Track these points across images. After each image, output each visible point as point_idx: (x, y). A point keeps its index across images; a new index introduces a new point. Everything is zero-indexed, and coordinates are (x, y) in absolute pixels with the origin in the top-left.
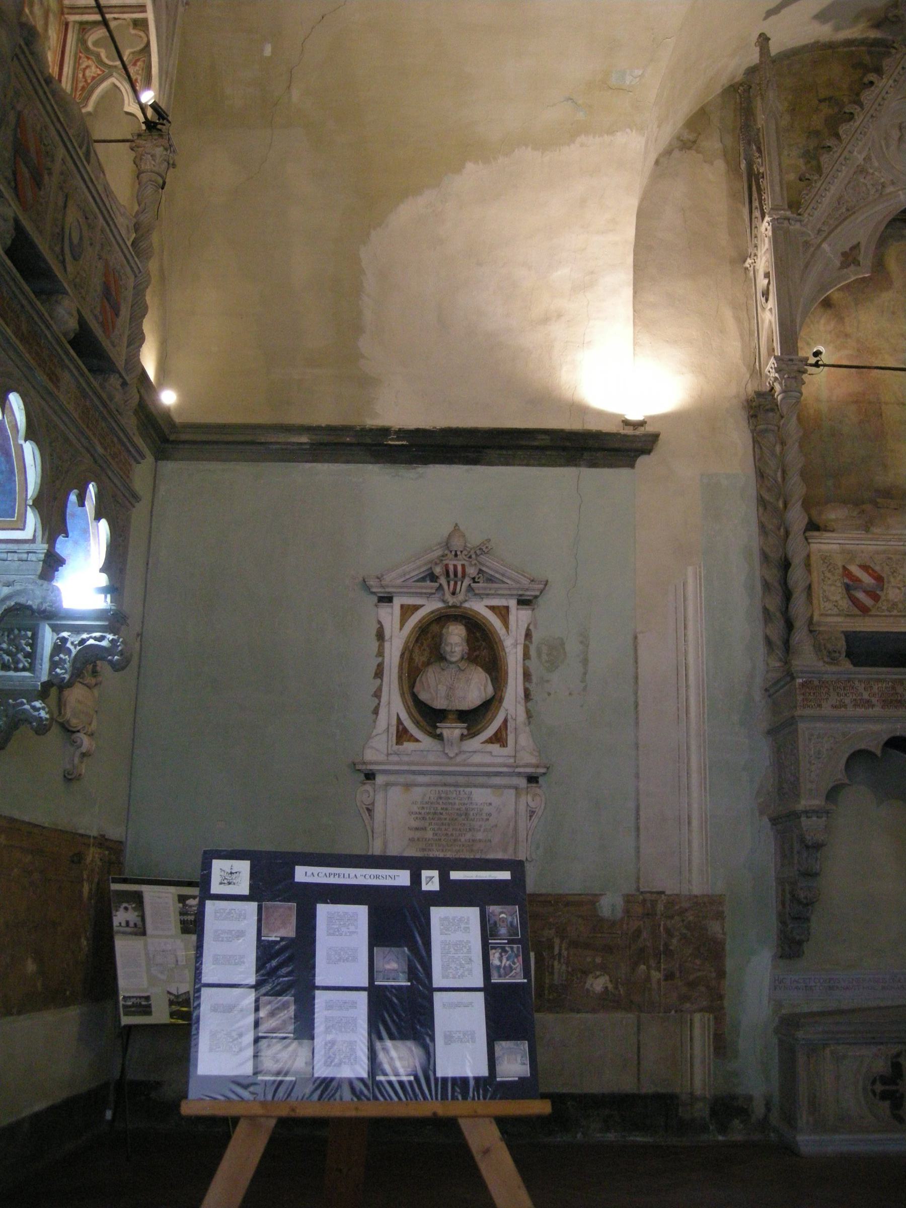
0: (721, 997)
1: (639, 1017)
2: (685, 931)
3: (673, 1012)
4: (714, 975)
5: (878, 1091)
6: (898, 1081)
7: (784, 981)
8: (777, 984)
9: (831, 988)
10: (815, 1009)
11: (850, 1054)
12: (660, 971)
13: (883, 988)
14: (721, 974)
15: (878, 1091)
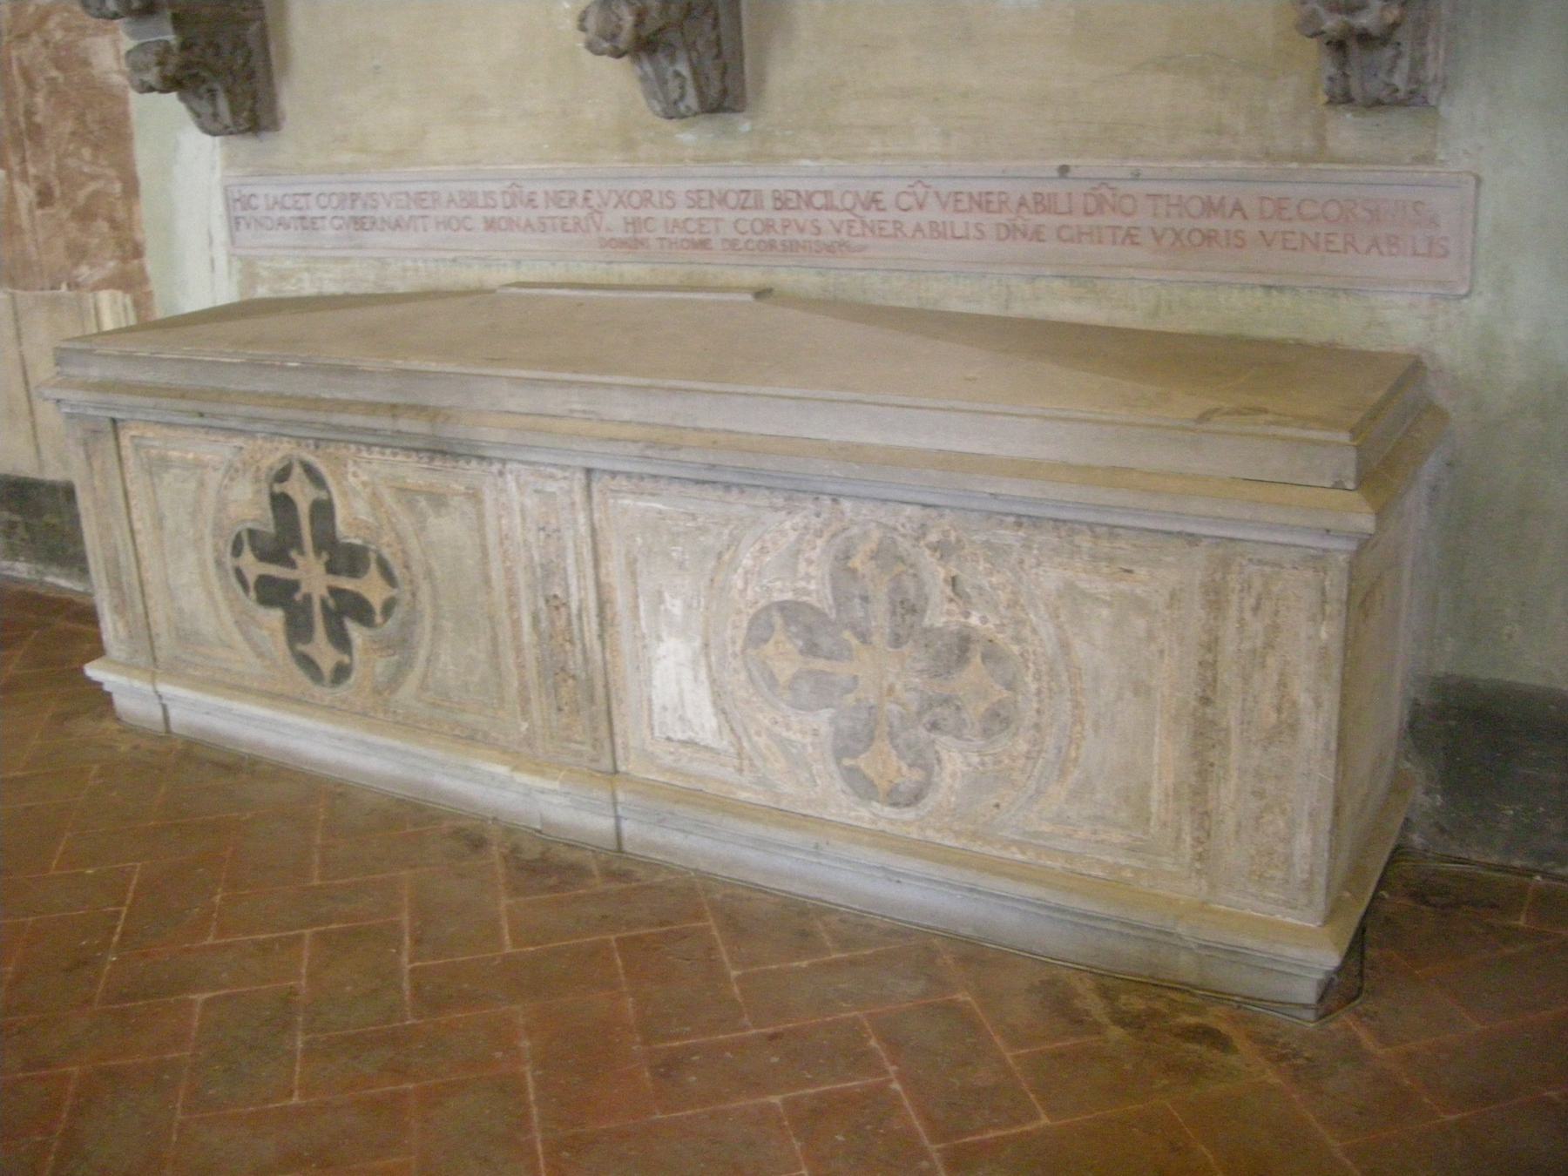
0: (138, 252)
1: (13, 296)
2: (54, 73)
3: (64, 287)
4: (118, 187)
5: (251, 579)
6: (293, 554)
7: (254, 202)
8: (239, 211)
9: (359, 223)
10: (330, 288)
11: (174, 454)
12: (27, 182)
13: (490, 225)
14: (131, 188)
15: (251, 579)
